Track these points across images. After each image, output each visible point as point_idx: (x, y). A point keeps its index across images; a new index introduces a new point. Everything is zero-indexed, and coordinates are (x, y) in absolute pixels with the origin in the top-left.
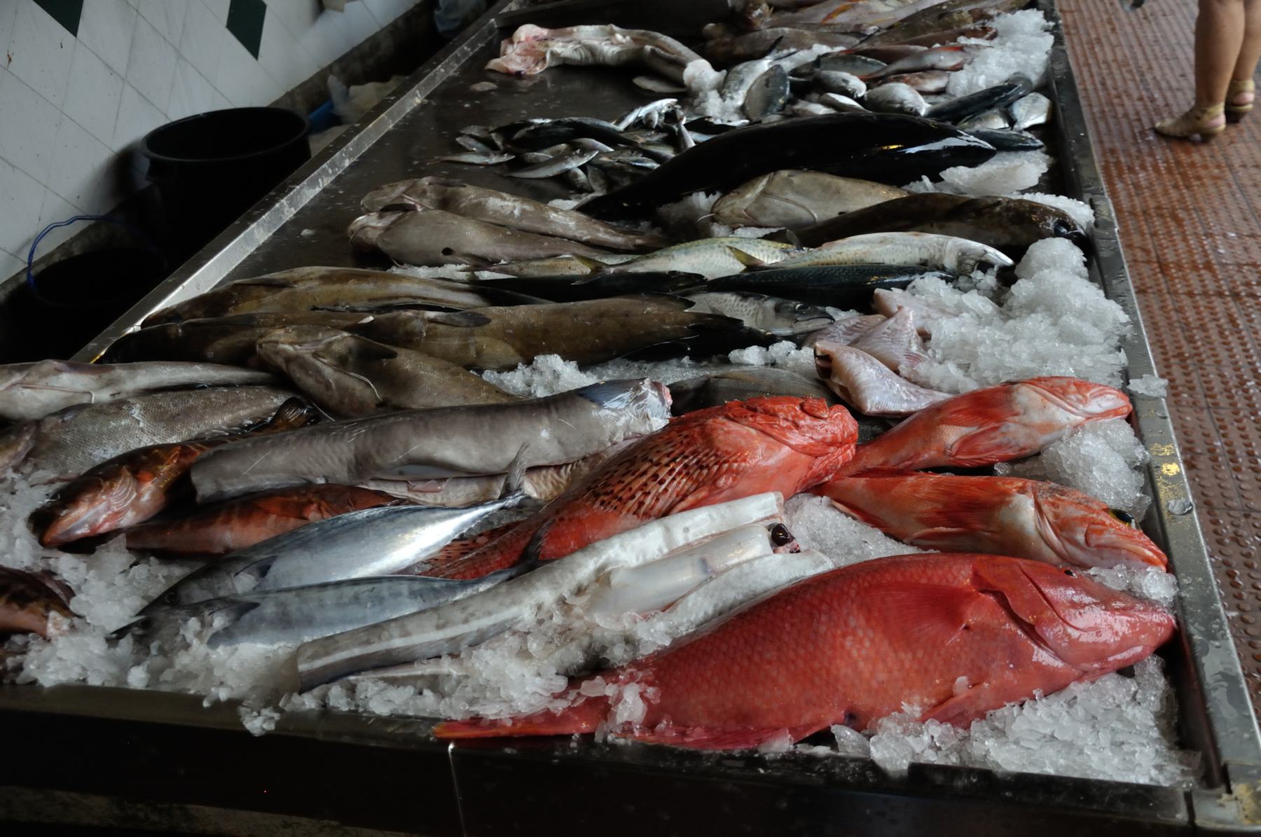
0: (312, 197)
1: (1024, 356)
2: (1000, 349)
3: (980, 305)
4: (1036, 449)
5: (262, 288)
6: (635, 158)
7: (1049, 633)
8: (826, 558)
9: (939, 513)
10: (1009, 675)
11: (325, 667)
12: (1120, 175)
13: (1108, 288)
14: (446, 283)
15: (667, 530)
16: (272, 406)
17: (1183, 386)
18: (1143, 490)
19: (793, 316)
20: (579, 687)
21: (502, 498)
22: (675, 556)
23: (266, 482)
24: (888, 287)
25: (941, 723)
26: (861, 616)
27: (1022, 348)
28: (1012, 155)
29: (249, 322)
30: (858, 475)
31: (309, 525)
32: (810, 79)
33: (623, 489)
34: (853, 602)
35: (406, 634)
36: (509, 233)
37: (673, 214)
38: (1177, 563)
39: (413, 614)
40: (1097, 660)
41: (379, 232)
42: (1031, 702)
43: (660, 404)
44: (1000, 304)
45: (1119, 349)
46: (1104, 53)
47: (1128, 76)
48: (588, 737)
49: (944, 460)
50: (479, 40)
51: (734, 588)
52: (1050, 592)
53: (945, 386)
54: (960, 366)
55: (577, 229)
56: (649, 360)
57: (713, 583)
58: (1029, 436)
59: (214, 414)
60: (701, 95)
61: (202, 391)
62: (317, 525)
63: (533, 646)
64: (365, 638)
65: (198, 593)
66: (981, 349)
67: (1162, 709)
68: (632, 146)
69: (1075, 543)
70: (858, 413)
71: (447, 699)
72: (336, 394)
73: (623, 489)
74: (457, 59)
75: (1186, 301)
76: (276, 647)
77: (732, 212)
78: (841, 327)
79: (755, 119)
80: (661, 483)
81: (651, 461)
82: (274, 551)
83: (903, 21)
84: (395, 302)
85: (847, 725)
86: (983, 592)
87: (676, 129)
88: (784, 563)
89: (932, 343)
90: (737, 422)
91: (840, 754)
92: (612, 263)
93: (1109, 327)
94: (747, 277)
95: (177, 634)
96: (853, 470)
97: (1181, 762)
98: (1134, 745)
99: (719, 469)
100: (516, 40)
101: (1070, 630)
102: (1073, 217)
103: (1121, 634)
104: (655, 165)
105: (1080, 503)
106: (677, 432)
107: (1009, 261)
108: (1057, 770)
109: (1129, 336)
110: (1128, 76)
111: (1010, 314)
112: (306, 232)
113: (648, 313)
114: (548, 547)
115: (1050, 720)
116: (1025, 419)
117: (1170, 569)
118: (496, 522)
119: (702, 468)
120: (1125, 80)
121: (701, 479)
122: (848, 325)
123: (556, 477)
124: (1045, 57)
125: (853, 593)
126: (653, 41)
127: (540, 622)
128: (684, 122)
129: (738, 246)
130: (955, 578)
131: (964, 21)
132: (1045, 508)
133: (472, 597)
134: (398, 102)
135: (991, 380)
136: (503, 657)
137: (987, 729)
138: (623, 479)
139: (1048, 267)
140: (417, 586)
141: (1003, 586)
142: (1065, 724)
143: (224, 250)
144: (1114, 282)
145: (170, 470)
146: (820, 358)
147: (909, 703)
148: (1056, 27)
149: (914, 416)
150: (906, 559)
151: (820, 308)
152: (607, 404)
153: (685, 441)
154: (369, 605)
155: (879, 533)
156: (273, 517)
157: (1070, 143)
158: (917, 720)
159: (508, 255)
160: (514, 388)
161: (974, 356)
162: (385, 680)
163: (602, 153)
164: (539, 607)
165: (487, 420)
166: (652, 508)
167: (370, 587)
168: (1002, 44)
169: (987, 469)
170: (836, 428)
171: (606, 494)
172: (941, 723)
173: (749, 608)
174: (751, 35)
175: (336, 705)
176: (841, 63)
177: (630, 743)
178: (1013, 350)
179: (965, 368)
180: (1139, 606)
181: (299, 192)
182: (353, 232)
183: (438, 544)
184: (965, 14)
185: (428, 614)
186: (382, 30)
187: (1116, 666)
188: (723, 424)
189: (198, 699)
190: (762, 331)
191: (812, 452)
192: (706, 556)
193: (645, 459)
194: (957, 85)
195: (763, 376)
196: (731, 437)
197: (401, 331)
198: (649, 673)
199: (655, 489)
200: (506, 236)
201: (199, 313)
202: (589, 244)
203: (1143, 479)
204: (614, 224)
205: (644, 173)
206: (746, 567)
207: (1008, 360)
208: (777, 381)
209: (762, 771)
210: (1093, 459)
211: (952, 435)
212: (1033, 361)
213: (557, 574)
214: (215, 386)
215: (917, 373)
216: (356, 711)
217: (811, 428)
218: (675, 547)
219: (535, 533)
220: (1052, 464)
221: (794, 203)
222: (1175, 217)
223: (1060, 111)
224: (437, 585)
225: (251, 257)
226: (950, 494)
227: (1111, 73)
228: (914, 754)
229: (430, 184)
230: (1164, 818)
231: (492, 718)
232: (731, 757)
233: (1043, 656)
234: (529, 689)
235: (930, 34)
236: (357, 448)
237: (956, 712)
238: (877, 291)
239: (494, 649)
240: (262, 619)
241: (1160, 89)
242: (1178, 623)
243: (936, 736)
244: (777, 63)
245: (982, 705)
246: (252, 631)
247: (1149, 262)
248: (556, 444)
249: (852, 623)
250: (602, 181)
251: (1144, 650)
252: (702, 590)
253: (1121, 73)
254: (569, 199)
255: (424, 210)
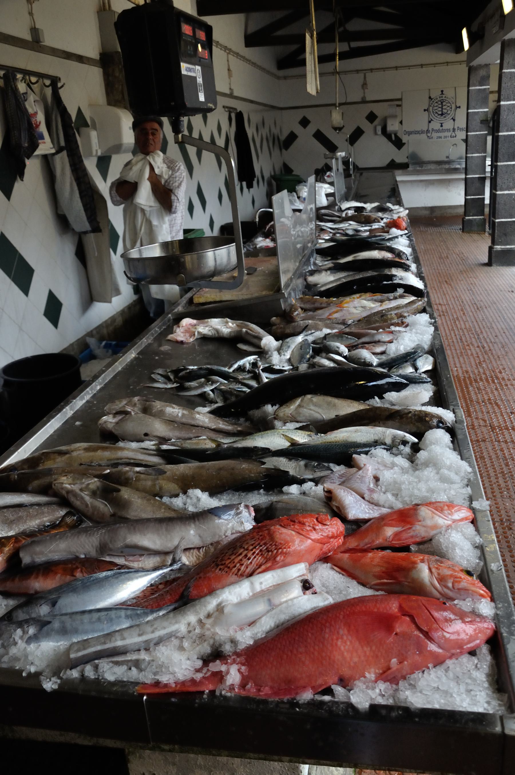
0: (81, 405)
1: (424, 490)
2: (412, 486)
3: (402, 463)
4: (430, 537)
5: (56, 454)
6: (237, 386)
7: (436, 635)
8: (329, 597)
9: (383, 572)
10: (417, 658)
11: (84, 656)
12: (471, 384)
13: (462, 454)
14: (145, 451)
15: (252, 583)
16: (59, 515)
17: (505, 488)
18: (480, 558)
19: (313, 469)
20: (208, 666)
21: (171, 565)
22: (256, 597)
23: (56, 557)
24: (359, 453)
25: (385, 682)
26: (345, 629)
27: (423, 486)
28: (417, 386)
29: (49, 472)
30: (344, 552)
31: (76, 580)
32: (321, 346)
33: (230, 563)
34: (341, 621)
35: (124, 639)
36: (176, 425)
37: (256, 415)
38: (495, 596)
39: (127, 628)
40: (459, 648)
41: (113, 425)
42: (428, 670)
43: (249, 516)
44: (412, 462)
45: (467, 485)
46: (460, 324)
47: (472, 336)
48: (212, 693)
49: (386, 544)
50: (163, 325)
51: (284, 614)
52: (436, 614)
53: (386, 505)
54: (393, 495)
55: (209, 423)
56: (243, 492)
57: (274, 611)
58: (426, 531)
59: (31, 520)
60: (269, 353)
61: (26, 508)
62: (80, 580)
63: (186, 644)
64: (103, 641)
65: (21, 615)
66: (403, 487)
67: (489, 671)
68: (237, 381)
69: (448, 588)
70: (344, 519)
71: (143, 672)
72: (91, 510)
73: (230, 563)
74: (152, 334)
75: (503, 445)
76: (59, 644)
77: (284, 415)
78: (337, 475)
79: (295, 366)
80: (249, 559)
81: (244, 548)
82: (59, 594)
83: (364, 318)
84: (120, 461)
85: (339, 685)
86: (404, 615)
87: (257, 372)
88: (309, 600)
89: (380, 482)
90: (286, 528)
91: (336, 700)
92: (226, 441)
93: (463, 474)
94: (292, 449)
95: (11, 637)
96: (342, 549)
97: (499, 700)
98: (476, 691)
99: (277, 552)
100: (181, 326)
101: (445, 634)
102: (445, 418)
103: (469, 634)
104: (248, 390)
105: (449, 568)
106: (257, 533)
107: (416, 440)
108: (440, 706)
109: (472, 479)
110: (472, 336)
111: (417, 467)
112: (78, 423)
113: (243, 468)
114: (194, 592)
115: (437, 680)
116: (424, 523)
117: (492, 600)
118: (168, 577)
119: (268, 551)
120: (470, 338)
121: (268, 557)
122: (340, 474)
123: (198, 553)
124: (431, 337)
125: (341, 617)
126: (246, 327)
127: (189, 632)
128: (261, 368)
129: (287, 434)
130: (390, 608)
131: (392, 318)
132: (434, 570)
133: (155, 619)
134: (123, 357)
135: (408, 502)
136: (171, 650)
137: (407, 685)
138: (230, 557)
139: (434, 444)
140: (129, 612)
141: (413, 612)
142: (444, 681)
143: (38, 433)
144: (465, 451)
145: (9, 550)
146: (327, 492)
147: (369, 673)
148: (435, 322)
149: (372, 521)
150: (367, 598)
151: (326, 464)
152: (222, 517)
153: (260, 538)
154: (105, 622)
155: (355, 582)
156: (59, 575)
157: (443, 380)
158: (373, 681)
159: (175, 437)
160: (178, 506)
161: (400, 490)
162: (113, 662)
163: (221, 384)
164: (189, 624)
165: (164, 525)
166: (244, 572)
167: (106, 613)
168: (411, 330)
169: (406, 549)
170: (333, 530)
171: (222, 565)
172: (385, 682)
173: (292, 625)
174: (293, 324)
175: (89, 675)
176: (336, 338)
177: (233, 695)
178: (418, 487)
179: (396, 495)
180: (478, 620)
181: (75, 403)
182: (100, 424)
183: (139, 589)
184: (393, 315)
185: (134, 628)
186: (117, 313)
187: (468, 650)
188: (279, 529)
189: (21, 671)
190: (299, 476)
191: (321, 542)
192: (271, 597)
193: (241, 547)
194: (390, 350)
195: (299, 501)
196: (282, 536)
197: (123, 478)
198: (243, 659)
199: (246, 562)
200: (174, 426)
201: (25, 467)
202: (214, 430)
203: (479, 553)
204: (227, 419)
205: (243, 394)
206: (290, 603)
207: (416, 492)
208: (306, 504)
209: (298, 710)
210: (456, 543)
211: (389, 532)
212: (428, 492)
213: (198, 607)
214: (32, 505)
215: (373, 499)
216: (98, 679)
217: (322, 530)
218: (255, 592)
219: (187, 585)
220: (437, 546)
221: (314, 411)
222: (497, 404)
223: (438, 364)
224: (139, 612)
225: (51, 436)
226: (388, 563)
227: (464, 334)
228: (372, 699)
229: (138, 400)
230: (490, 730)
231: (165, 682)
232: (283, 702)
233: (432, 647)
234: (184, 667)
235: (378, 324)
236: (100, 540)
237: (392, 676)
238: (354, 456)
239: (166, 646)
240: (52, 630)
241: (487, 342)
242: (496, 627)
243: (382, 689)
244: (306, 338)
245: (404, 673)
246: (48, 635)
247: (486, 426)
248: (198, 537)
249: (341, 632)
250: (221, 398)
251: (480, 642)
252: (268, 615)
253: (469, 334)
254: (205, 407)
255: (135, 414)
